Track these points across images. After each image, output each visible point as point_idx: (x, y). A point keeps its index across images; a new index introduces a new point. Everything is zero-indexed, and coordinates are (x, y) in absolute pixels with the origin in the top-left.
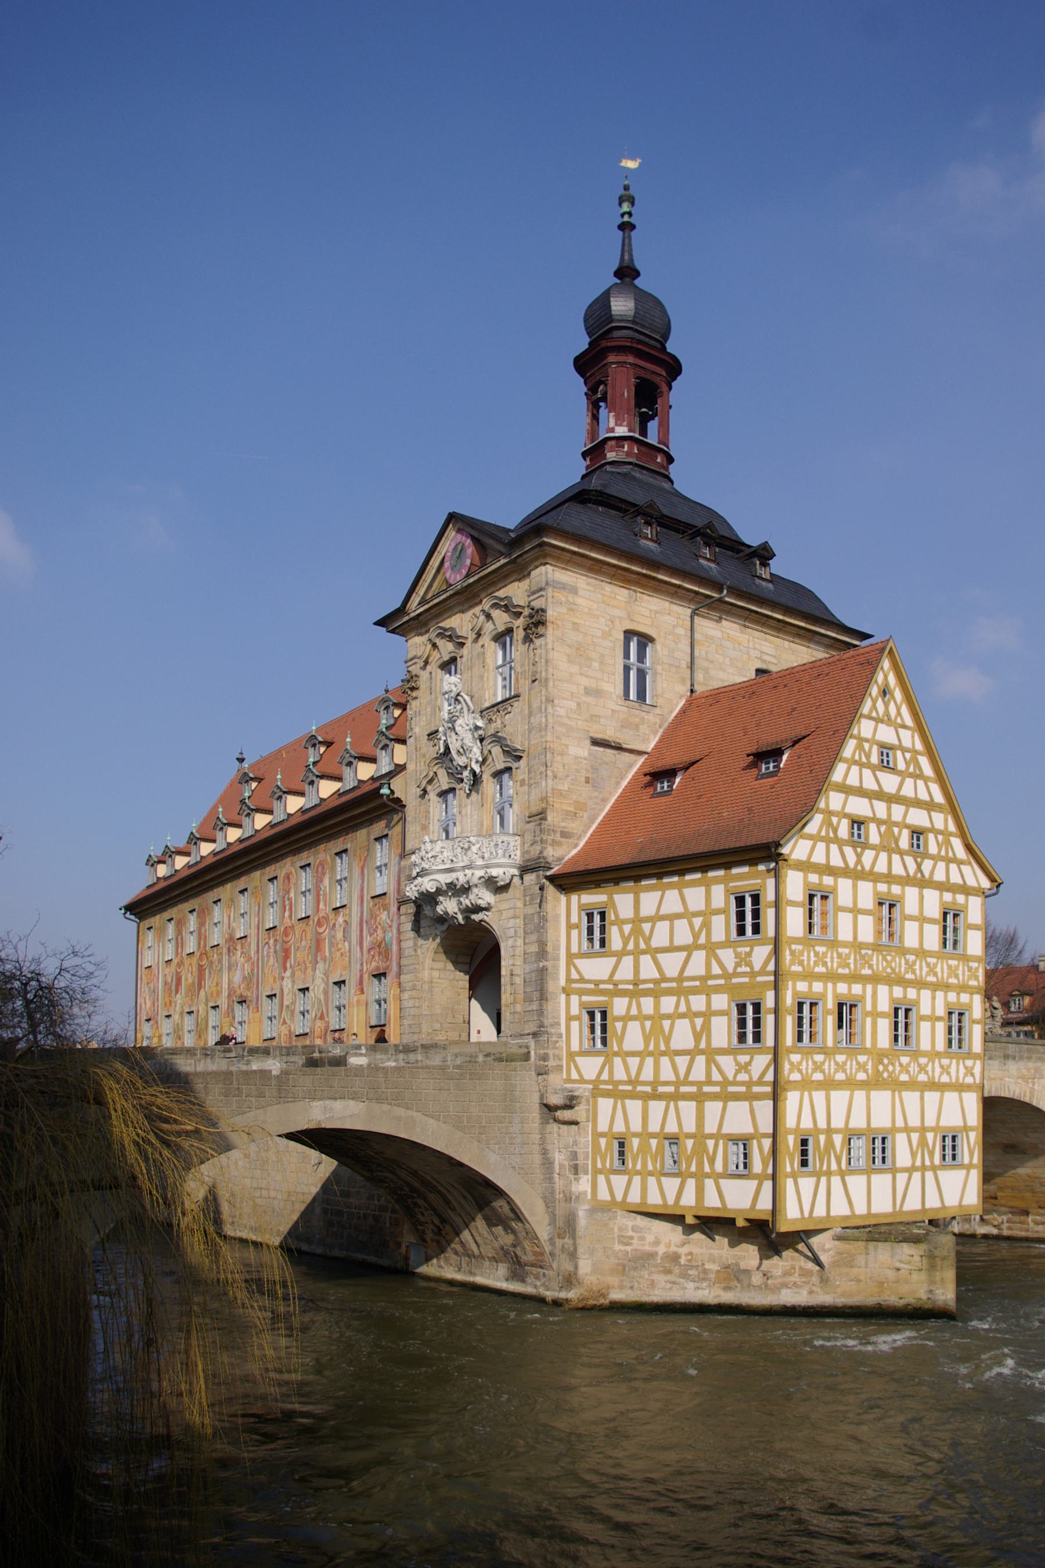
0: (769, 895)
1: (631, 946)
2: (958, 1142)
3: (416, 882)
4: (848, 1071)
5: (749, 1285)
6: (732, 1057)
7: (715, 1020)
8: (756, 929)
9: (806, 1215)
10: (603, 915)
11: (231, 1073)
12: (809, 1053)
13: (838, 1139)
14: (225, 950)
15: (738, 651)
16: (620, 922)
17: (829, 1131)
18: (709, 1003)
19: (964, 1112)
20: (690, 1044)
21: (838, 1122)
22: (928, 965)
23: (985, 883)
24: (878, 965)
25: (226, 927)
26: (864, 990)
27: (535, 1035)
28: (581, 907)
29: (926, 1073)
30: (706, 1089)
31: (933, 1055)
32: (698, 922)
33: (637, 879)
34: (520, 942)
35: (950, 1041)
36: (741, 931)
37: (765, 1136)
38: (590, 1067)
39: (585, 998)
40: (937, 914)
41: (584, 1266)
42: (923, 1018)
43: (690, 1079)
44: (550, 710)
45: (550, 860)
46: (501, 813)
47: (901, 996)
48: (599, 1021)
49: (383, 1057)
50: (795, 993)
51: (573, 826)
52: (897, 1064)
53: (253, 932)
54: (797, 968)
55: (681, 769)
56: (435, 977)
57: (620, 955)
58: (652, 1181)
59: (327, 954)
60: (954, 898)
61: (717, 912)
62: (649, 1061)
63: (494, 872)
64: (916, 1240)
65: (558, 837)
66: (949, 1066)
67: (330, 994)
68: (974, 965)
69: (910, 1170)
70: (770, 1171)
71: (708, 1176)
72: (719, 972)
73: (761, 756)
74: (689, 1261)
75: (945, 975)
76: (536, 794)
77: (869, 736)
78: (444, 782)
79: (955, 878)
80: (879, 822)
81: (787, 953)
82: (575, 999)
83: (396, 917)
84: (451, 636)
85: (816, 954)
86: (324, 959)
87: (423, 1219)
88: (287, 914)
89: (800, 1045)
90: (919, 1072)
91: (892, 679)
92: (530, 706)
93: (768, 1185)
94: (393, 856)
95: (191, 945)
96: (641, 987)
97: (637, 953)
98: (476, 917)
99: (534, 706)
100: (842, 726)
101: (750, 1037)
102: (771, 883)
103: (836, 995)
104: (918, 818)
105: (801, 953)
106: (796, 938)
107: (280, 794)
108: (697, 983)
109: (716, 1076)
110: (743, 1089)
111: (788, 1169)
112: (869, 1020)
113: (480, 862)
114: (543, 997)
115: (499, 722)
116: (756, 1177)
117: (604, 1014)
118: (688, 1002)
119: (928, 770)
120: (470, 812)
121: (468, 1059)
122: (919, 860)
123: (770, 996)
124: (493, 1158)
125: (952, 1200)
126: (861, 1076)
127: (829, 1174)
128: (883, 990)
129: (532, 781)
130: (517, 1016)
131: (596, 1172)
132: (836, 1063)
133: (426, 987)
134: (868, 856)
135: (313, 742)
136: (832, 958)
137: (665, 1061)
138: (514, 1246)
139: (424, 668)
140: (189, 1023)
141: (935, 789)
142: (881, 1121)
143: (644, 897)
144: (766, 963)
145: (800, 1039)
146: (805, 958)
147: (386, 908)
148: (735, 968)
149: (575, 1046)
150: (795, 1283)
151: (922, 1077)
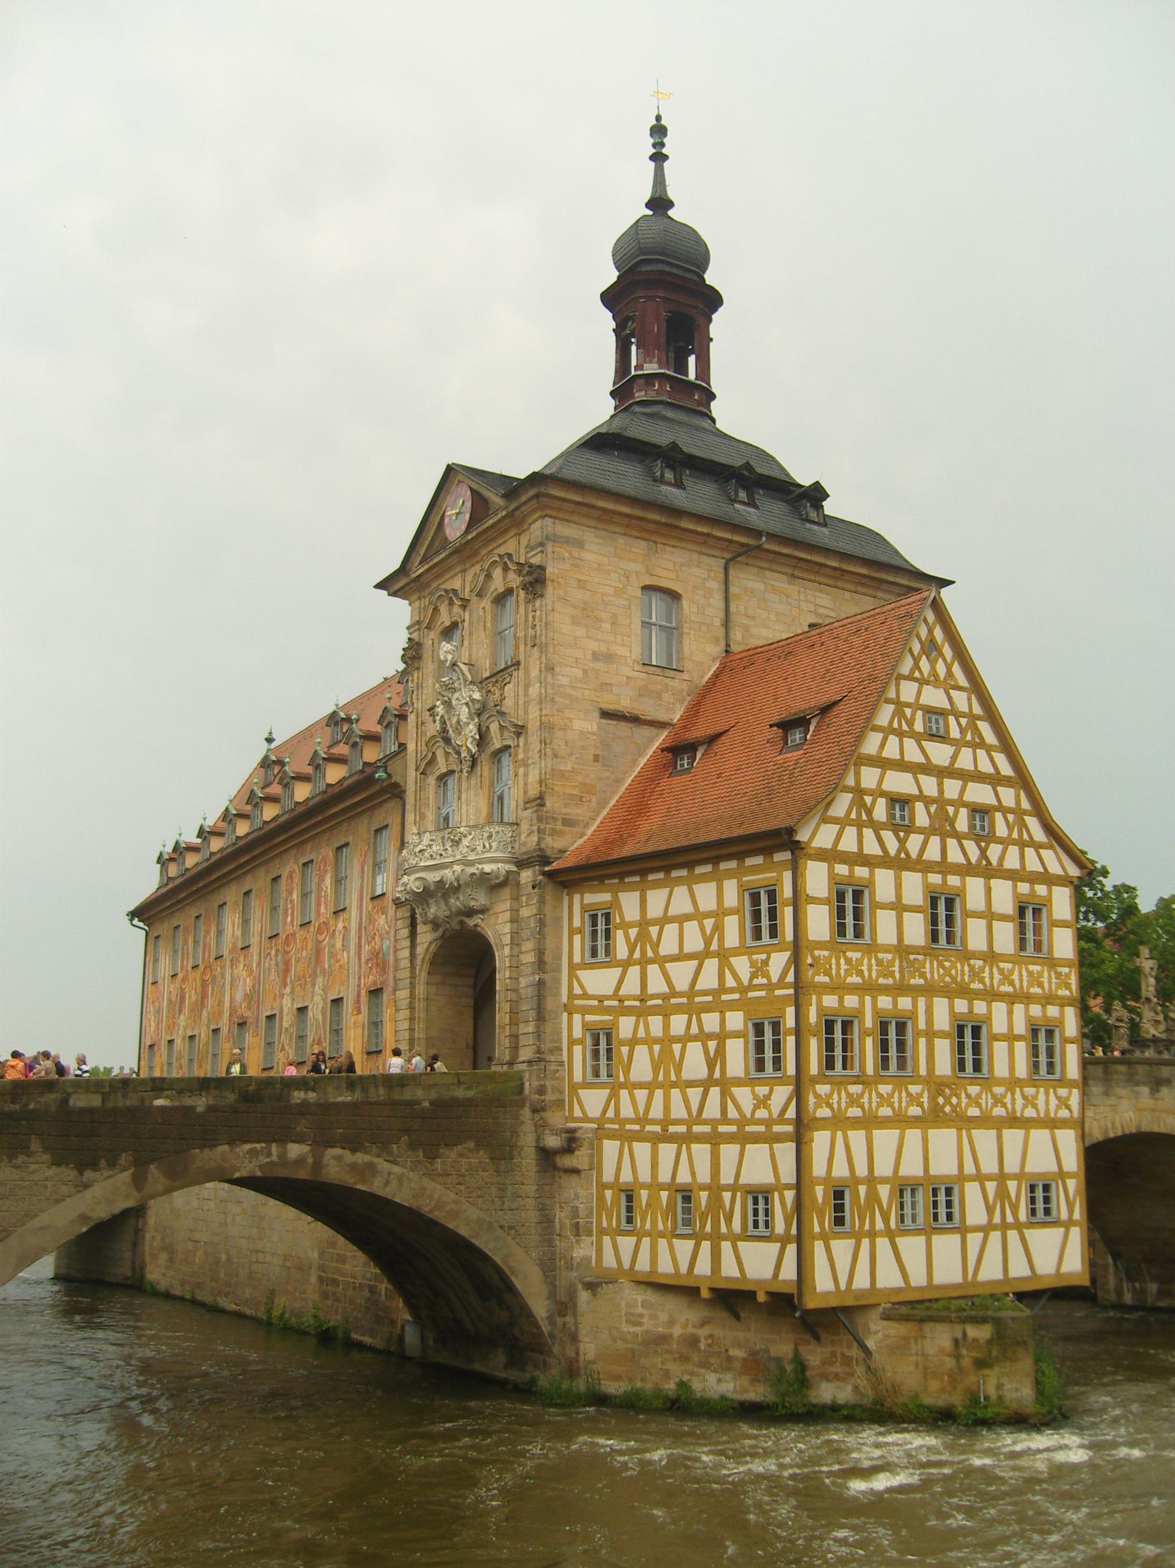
1: (637, 955)
2: (1053, 1194)
4: (896, 1105)
6: (746, 1090)
8: (773, 932)
9: (843, 1286)
10: (607, 917)
12: (842, 1083)
13: (884, 1191)
14: (228, 963)
16: (626, 926)
17: (872, 1180)
18: (723, 1022)
19: (1058, 1154)
20: (703, 1073)
21: (884, 1168)
22: (1001, 971)
24: (932, 973)
26: (915, 1005)
28: (584, 909)
29: (1004, 1105)
30: (722, 1129)
31: (1013, 1083)
33: (644, 873)
36: (757, 935)
37: (788, 1187)
38: (593, 1101)
39: (588, 1018)
42: (996, 1038)
44: (550, 679)
45: (549, 853)
46: (501, 798)
47: (966, 1010)
48: (603, 1043)
50: (820, 1009)
51: (578, 812)
52: (963, 1095)
54: (822, 979)
57: (626, 964)
60: (1032, 889)
62: (659, 1094)
63: (488, 868)
65: (559, 827)
66: (1035, 1097)
68: (1065, 970)
69: (986, 1229)
70: (794, 1231)
71: (725, 1238)
72: (733, 984)
75: (1025, 984)
76: (533, 777)
85: (848, 961)
86: (323, 972)
88: (289, 919)
90: (995, 1105)
93: (791, 1249)
96: (649, 1003)
97: (644, 962)
98: (471, 922)
100: (877, 685)
102: (787, 876)
103: (876, 1011)
104: (980, 794)
106: (819, 943)
108: (710, 998)
109: (732, 1113)
110: (762, 1128)
111: (817, 1229)
112: (922, 1041)
114: (541, 1017)
117: (609, 1036)
122: (983, 844)
123: (790, 1012)
126: (914, 1111)
127: (872, 1234)
128: (941, 1005)
132: (880, 1095)
134: (914, 842)
142: (944, 1165)
147: (384, 911)
151: (998, 1111)
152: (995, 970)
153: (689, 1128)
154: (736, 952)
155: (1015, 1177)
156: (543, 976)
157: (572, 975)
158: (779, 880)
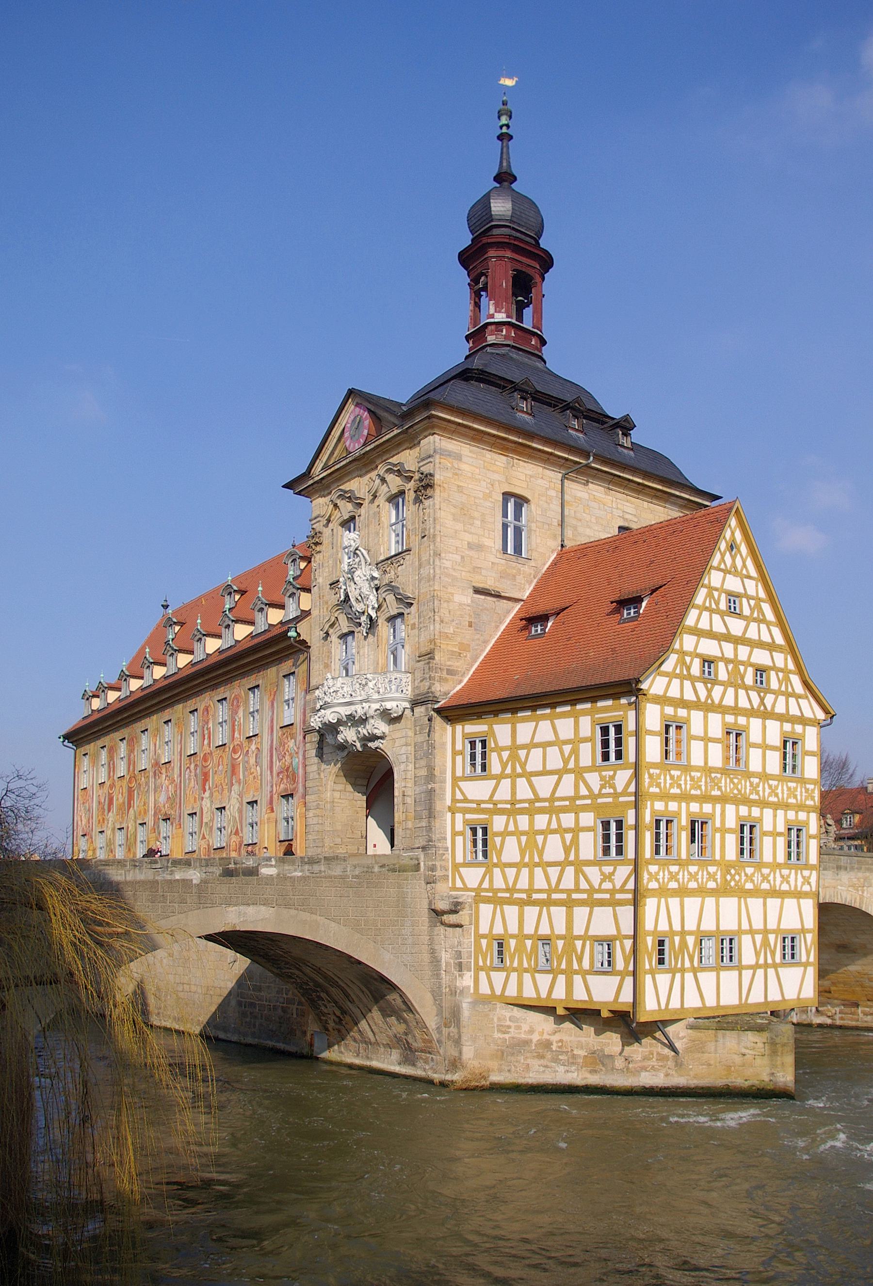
0: (631, 726)
1: (508, 770)
2: (797, 941)
3: (319, 714)
4: (700, 880)
5: (613, 1069)
7: (582, 836)
8: (619, 755)
9: (663, 1007)
10: (484, 743)
11: (157, 882)
13: (691, 940)
14: (151, 774)
15: (603, 511)
16: (499, 749)
17: (683, 933)
19: (801, 916)
20: (561, 857)
21: (691, 926)
22: (770, 786)
23: (821, 715)
24: (726, 787)
25: (152, 753)
27: (424, 848)
28: (465, 736)
29: (769, 882)
30: (575, 896)
31: (775, 866)
32: (567, 749)
33: (514, 711)
34: (411, 767)
35: (789, 854)
37: (627, 937)
38: (473, 876)
39: (468, 816)
40: (778, 743)
41: (468, 1053)
42: (766, 834)
43: (561, 887)
44: (437, 562)
46: (394, 653)
47: (747, 814)
48: (481, 836)
49: (290, 867)
50: (653, 811)
51: (457, 664)
52: (743, 874)
53: (176, 758)
54: (654, 790)
55: (553, 614)
56: (336, 797)
57: (499, 778)
58: (527, 977)
59: (241, 777)
60: (793, 728)
61: (585, 740)
62: (525, 871)
63: (388, 705)
64: (760, 1029)
65: (444, 675)
66: (788, 876)
67: (244, 812)
68: (811, 787)
69: (755, 967)
70: (631, 968)
71: (576, 972)
73: (623, 603)
74: (560, 1047)
75: (785, 796)
77: (719, 586)
78: (344, 626)
79: (794, 711)
80: (728, 661)
81: (646, 776)
82: (459, 817)
83: (302, 745)
84: (349, 497)
85: (672, 777)
86: (239, 782)
87: (326, 1011)
88: (206, 742)
89: (657, 857)
91: (738, 536)
92: (419, 560)
93: (629, 980)
94: (299, 691)
95: (122, 769)
96: (517, 806)
97: (514, 776)
98: (372, 745)
99: (423, 559)
101: (613, 850)
102: (632, 714)
103: (689, 813)
104: (761, 657)
105: (659, 776)
106: (654, 764)
107: (200, 636)
108: (567, 803)
109: (584, 885)
110: (607, 896)
111: (647, 967)
112: (718, 835)
113: (376, 696)
114: (431, 815)
115: (393, 573)
116: (619, 973)
117: (485, 830)
118: (558, 820)
119: (770, 616)
120: (366, 652)
121: (365, 869)
122: (762, 694)
123: (631, 813)
124: (387, 956)
125: (791, 994)
126: (711, 885)
127: (683, 970)
128: (730, 809)
129: (421, 625)
130: (408, 832)
131: (478, 969)
132: (690, 873)
133: (328, 806)
134: (717, 691)
135: (228, 591)
136: (686, 780)
137: (538, 871)
138: (406, 1034)
139: (326, 526)
140: (120, 838)
141: (776, 632)
142: (729, 924)
143: (520, 726)
144: (628, 785)
145: (657, 852)
146: (662, 781)
147: (293, 736)
148: (600, 790)
149: (459, 859)
150: (653, 1067)
151: (765, 886)
152: (766, 786)
153: (549, 896)
154: (589, 769)
155: (773, 931)
156: (433, 785)
157: (455, 785)
158: (626, 717)
